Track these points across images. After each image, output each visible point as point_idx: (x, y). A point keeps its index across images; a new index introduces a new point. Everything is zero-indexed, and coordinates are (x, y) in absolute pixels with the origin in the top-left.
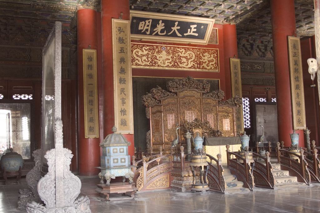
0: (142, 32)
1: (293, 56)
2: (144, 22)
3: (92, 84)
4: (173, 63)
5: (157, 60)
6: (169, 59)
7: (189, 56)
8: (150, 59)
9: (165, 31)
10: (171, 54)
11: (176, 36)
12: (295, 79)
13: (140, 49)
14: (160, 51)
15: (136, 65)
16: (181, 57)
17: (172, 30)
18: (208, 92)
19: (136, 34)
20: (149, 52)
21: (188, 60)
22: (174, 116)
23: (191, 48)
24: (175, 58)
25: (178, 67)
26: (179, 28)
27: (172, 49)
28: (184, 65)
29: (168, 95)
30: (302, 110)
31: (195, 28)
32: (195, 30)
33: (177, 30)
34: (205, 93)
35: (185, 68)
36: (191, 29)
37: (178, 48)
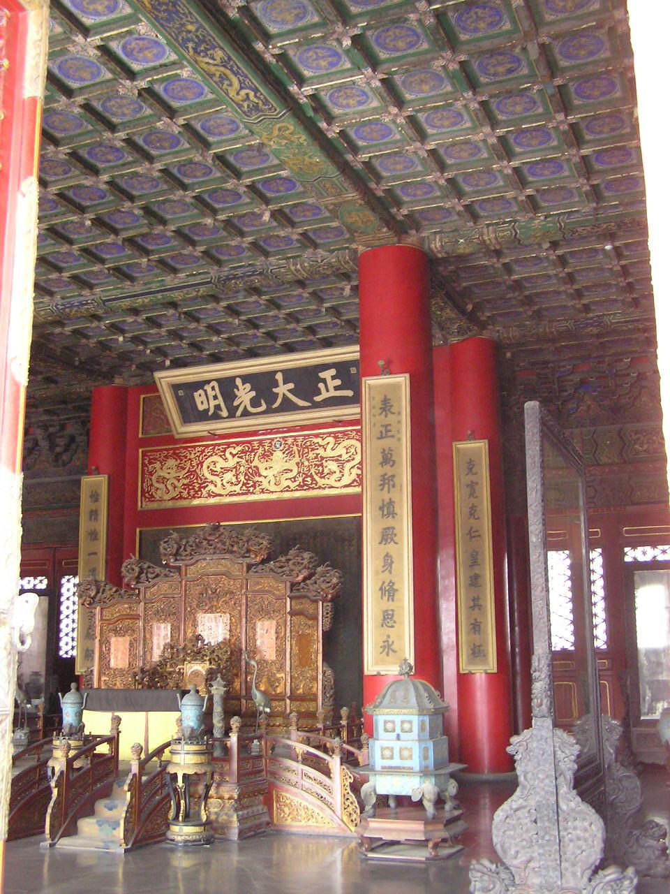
0: (210, 413)
1: (379, 438)
2: (201, 391)
3: (96, 553)
4: (301, 479)
5: (260, 476)
6: (291, 471)
7: (347, 453)
8: (242, 478)
9: (263, 402)
10: (297, 455)
11: (296, 408)
12: (381, 508)
13: (221, 456)
14: (268, 451)
15: (209, 495)
16: (322, 458)
17: (278, 394)
18: (263, 562)
19: (200, 421)
20: (240, 460)
21: (341, 467)
22: (169, 628)
23: (351, 431)
24: (306, 463)
25: (313, 488)
26: (291, 386)
27: (299, 443)
28: (331, 481)
29: (157, 576)
30: (402, 608)
31: (333, 378)
32: (338, 382)
33: (290, 391)
34: (253, 565)
35: (333, 487)
36: (324, 381)
37: (317, 436)
